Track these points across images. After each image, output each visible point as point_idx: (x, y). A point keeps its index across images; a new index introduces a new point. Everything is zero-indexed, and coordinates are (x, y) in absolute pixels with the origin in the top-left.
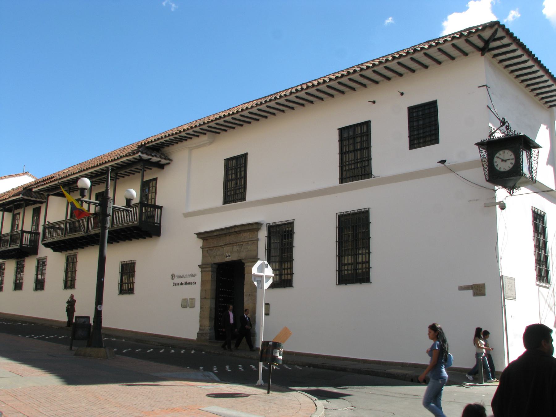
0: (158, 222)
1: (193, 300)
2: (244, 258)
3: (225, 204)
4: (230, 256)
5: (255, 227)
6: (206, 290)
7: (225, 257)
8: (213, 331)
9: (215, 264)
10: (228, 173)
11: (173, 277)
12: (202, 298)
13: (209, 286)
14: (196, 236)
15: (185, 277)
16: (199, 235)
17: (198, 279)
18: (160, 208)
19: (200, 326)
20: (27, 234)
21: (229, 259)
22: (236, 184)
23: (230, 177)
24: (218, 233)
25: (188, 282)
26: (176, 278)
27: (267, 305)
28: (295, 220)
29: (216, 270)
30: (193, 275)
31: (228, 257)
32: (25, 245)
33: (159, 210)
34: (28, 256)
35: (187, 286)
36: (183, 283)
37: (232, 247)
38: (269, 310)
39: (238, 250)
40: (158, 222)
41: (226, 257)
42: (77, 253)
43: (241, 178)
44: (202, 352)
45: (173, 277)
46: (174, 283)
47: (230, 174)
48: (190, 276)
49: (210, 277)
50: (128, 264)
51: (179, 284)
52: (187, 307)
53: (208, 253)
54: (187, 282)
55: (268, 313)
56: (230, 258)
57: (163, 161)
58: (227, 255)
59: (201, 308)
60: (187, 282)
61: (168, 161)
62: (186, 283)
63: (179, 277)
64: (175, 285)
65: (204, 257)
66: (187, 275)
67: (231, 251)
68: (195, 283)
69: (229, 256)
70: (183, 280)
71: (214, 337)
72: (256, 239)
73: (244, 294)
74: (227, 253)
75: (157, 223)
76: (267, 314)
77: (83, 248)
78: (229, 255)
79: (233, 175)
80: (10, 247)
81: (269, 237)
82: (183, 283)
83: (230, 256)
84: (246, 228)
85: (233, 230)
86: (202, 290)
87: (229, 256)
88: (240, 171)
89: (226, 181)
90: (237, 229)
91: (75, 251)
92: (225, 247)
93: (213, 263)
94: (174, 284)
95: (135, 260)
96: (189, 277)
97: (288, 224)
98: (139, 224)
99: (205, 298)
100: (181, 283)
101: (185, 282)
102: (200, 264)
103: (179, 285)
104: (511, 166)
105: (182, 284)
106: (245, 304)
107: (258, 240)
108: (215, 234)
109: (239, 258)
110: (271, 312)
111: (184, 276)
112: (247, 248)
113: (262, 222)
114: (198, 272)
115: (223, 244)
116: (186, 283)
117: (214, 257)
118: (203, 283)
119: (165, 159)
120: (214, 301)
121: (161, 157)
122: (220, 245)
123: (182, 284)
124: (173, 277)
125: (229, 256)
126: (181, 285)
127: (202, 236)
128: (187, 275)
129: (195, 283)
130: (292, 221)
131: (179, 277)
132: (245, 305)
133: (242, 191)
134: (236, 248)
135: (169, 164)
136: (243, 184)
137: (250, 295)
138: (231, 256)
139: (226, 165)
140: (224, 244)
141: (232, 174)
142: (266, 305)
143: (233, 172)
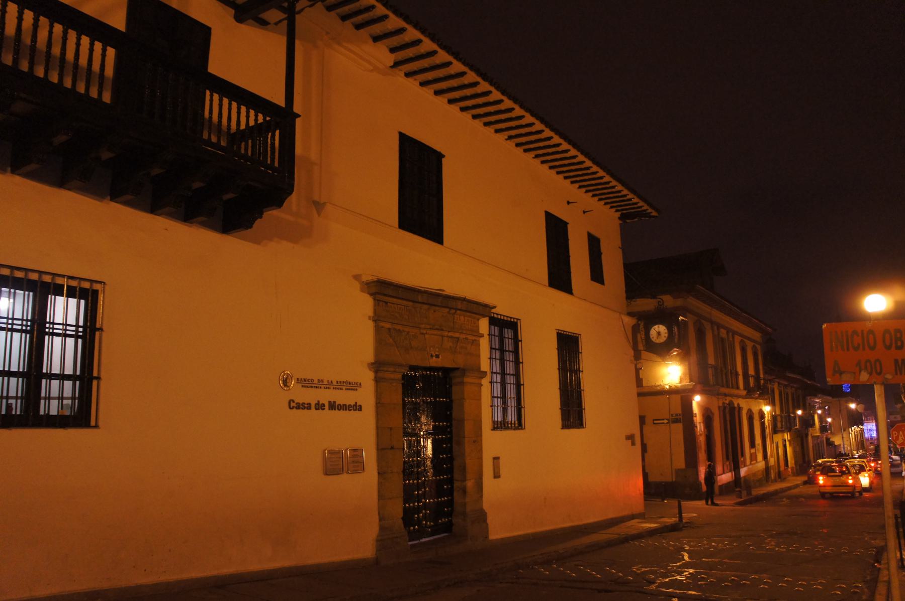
4: (439, 357)
6: (391, 429)
7: (430, 356)
12: (383, 449)
17: (366, 396)
19: (380, 520)
27: (496, 459)
30: (353, 386)
31: (434, 358)
36: (323, 405)
39: (450, 347)
41: (432, 356)
59: (380, 474)
62: (333, 406)
65: (380, 343)
66: (335, 383)
69: (437, 356)
70: (325, 396)
74: (432, 349)
76: (497, 476)
83: (439, 355)
96: (342, 389)
99: (392, 448)
101: (330, 402)
104: (665, 339)
105: (319, 406)
110: (503, 471)
111: (325, 382)
114: (367, 378)
116: (333, 406)
118: (380, 406)
123: (319, 406)
125: (437, 356)
129: (360, 408)
131: (305, 383)
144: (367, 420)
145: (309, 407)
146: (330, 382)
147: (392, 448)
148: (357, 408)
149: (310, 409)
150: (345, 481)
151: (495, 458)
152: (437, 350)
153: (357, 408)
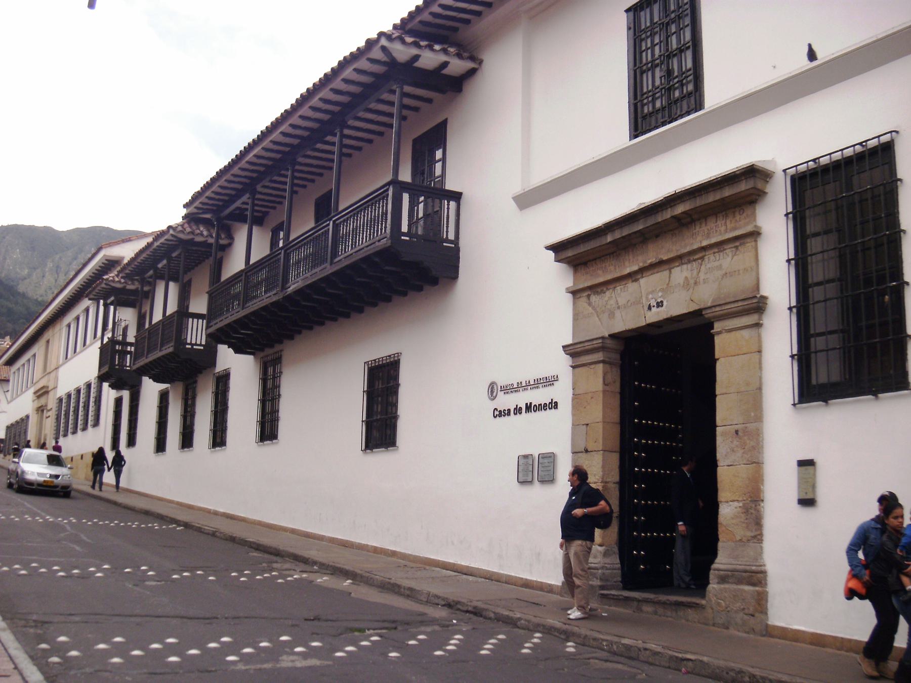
0: (451, 237)
1: (549, 459)
2: (709, 304)
3: (636, 136)
5: (743, 186)
7: (646, 308)
8: (615, 560)
9: (612, 336)
10: (641, 47)
11: (492, 392)
13: (596, 412)
14: (551, 254)
15: (526, 389)
16: (558, 248)
17: (563, 392)
18: (457, 197)
20: (195, 320)
21: (658, 313)
22: (669, 72)
23: (647, 57)
24: (618, 234)
25: (535, 402)
26: (501, 394)
28: (897, 132)
29: (618, 356)
30: (550, 381)
31: (654, 310)
32: (196, 344)
33: (453, 204)
34: (201, 373)
35: (532, 415)
37: (668, 271)
38: (814, 487)
39: (686, 278)
40: (451, 237)
41: (650, 308)
42: (281, 351)
43: (681, 50)
44: (567, 640)
45: (492, 391)
46: (496, 409)
47: (647, 49)
48: (540, 385)
49: (601, 380)
50: (383, 366)
51: (509, 410)
52: (531, 482)
53: (590, 304)
54: (531, 403)
55: (809, 496)
56: (660, 309)
57: (457, 66)
58: (653, 303)
60: (531, 403)
61: (470, 65)
62: (529, 408)
63: (508, 389)
64: (500, 415)
65: (577, 317)
66: (532, 383)
67: (665, 286)
68: (556, 403)
69: (660, 304)
70: (521, 399)
71: (620, 579)
72: (749, 228)
73: (715, 431)
75: (447, 241)
77: (291, 338)
78: (659, 300)
79: (657, 48)
80: (161, 350)
81: (798, 217)
82: (521, 408)
83: (662, 302)
84: (712, 197)
85: (667, 214)
86: (575, 425)
87: (658, 303)
88: (680, 29)
89: (635, 71)
90: (680, 209)
91: (278, 347)
92: (643, 277)
93: (606, 335)
94: (497, 413)
95: (399, 354)
97: (874, 152)
98: (390, 241)
99: (587, 451)
100: (515, 409)
101: (527, 404)
102: (569, 341)
103: (509, 414)
106: (720, 463)
107: (755, 234)
108: (609, 238)
109: (693, 307)
112: (720, 267)
113: (769, 167)
114: (561, 365)
115: (635, 268)
116: (529, 408)
117: (612, 315)
118: (578, 400)
119: (459, 56)
120: (615, 459)
121: (445, 51)
122: (628, 271)
123: (518, 411)
124: (492, 392)
126: (515, 414)
127: (570, 253)
128: (532, 383)
130: (886, 138)
131: (508, 389)
132: (719, 469)
133: (691, 87)
134: (680, 274)
135: (472, 72)
136: (690, 64)
137: (737, 432)
138: (665, 303)
139: (632, 26)
140: (641, 265)
141: (653, 45)
142: (803, 468)
143: (657, 40)
144: (562, 419)
145: (508, 413)
146: (527, 382)
147: (587, 451)
148: (554, 405)
149: (510, 415)
150: (537, 491)
151: (802, 463)
152: (660, 294)
153: (554, 405)
